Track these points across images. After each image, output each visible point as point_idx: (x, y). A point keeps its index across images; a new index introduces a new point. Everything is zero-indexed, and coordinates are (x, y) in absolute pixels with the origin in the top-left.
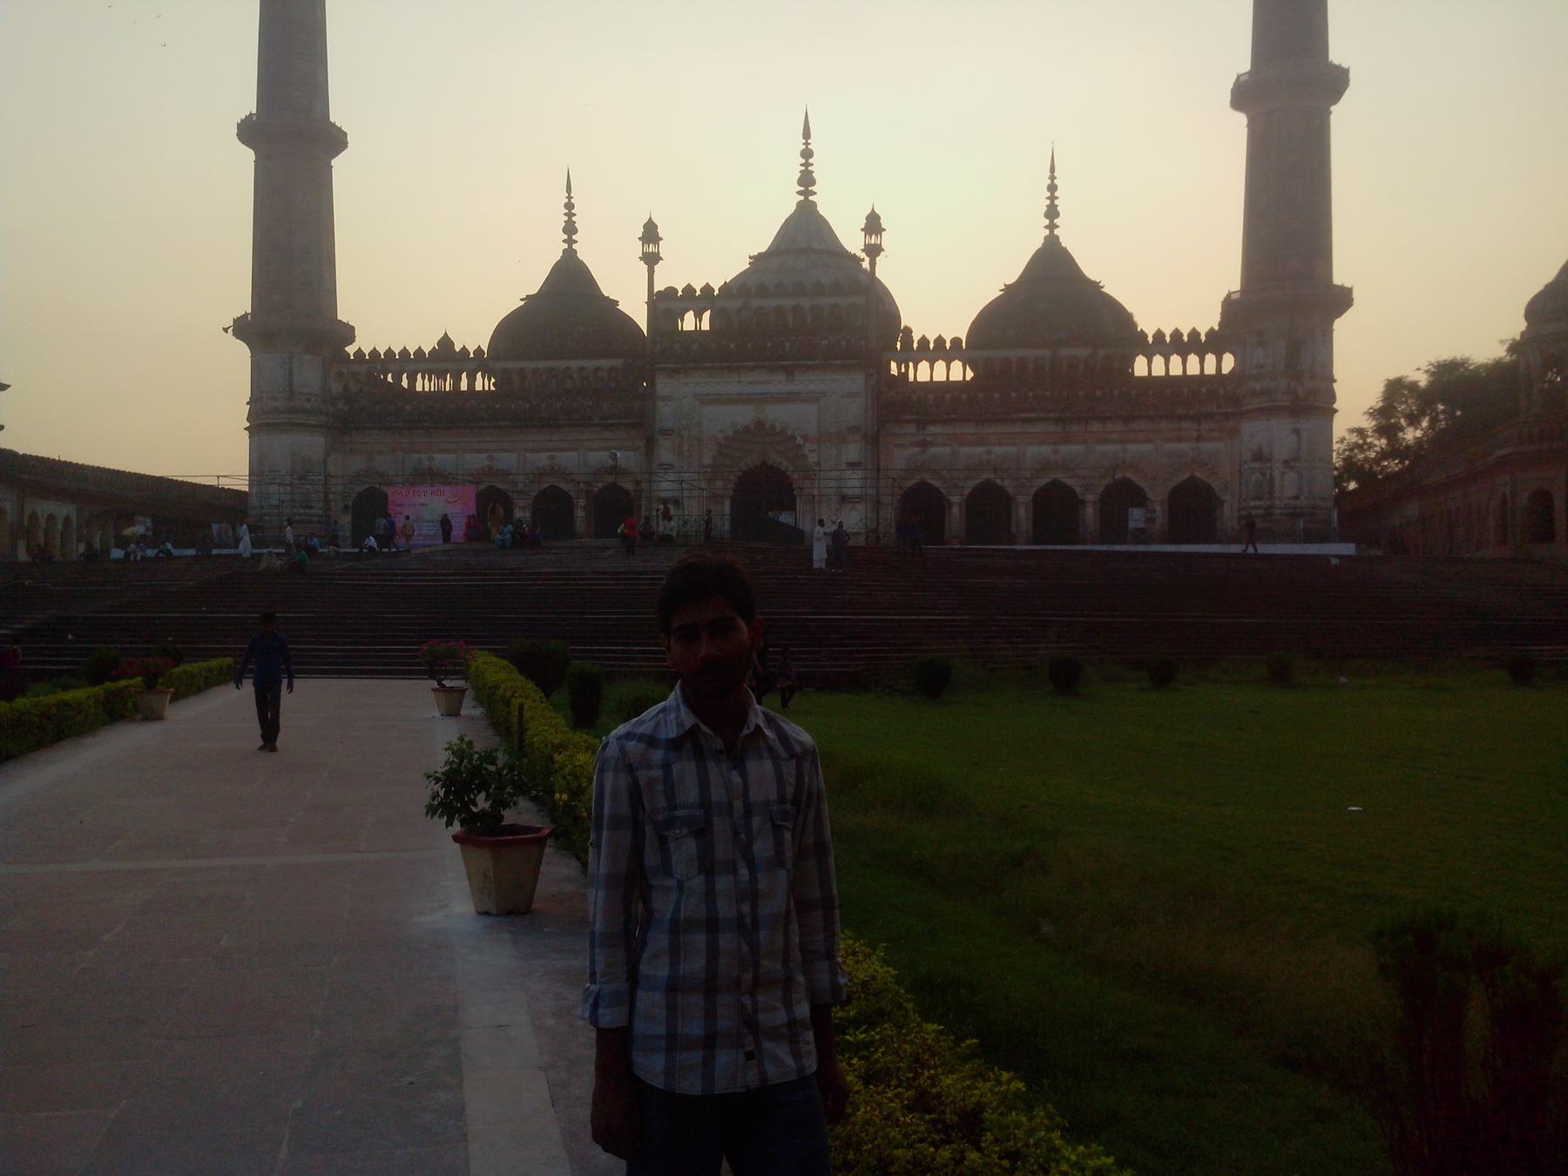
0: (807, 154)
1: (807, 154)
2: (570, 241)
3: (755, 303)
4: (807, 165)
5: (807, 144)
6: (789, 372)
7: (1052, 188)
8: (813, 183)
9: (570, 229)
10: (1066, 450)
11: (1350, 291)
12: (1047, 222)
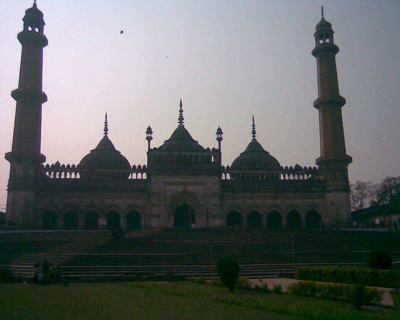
0: (181, 111)
1: (181, 111)
2: (106, 134)
3: (183, 154)
4: (181, 114)
5: (181, 108)
6: (194, 175)
7: (254, 125)
8: (183, 119)
9: (106, 130)
10: (278, 201)
11: (351, 158)
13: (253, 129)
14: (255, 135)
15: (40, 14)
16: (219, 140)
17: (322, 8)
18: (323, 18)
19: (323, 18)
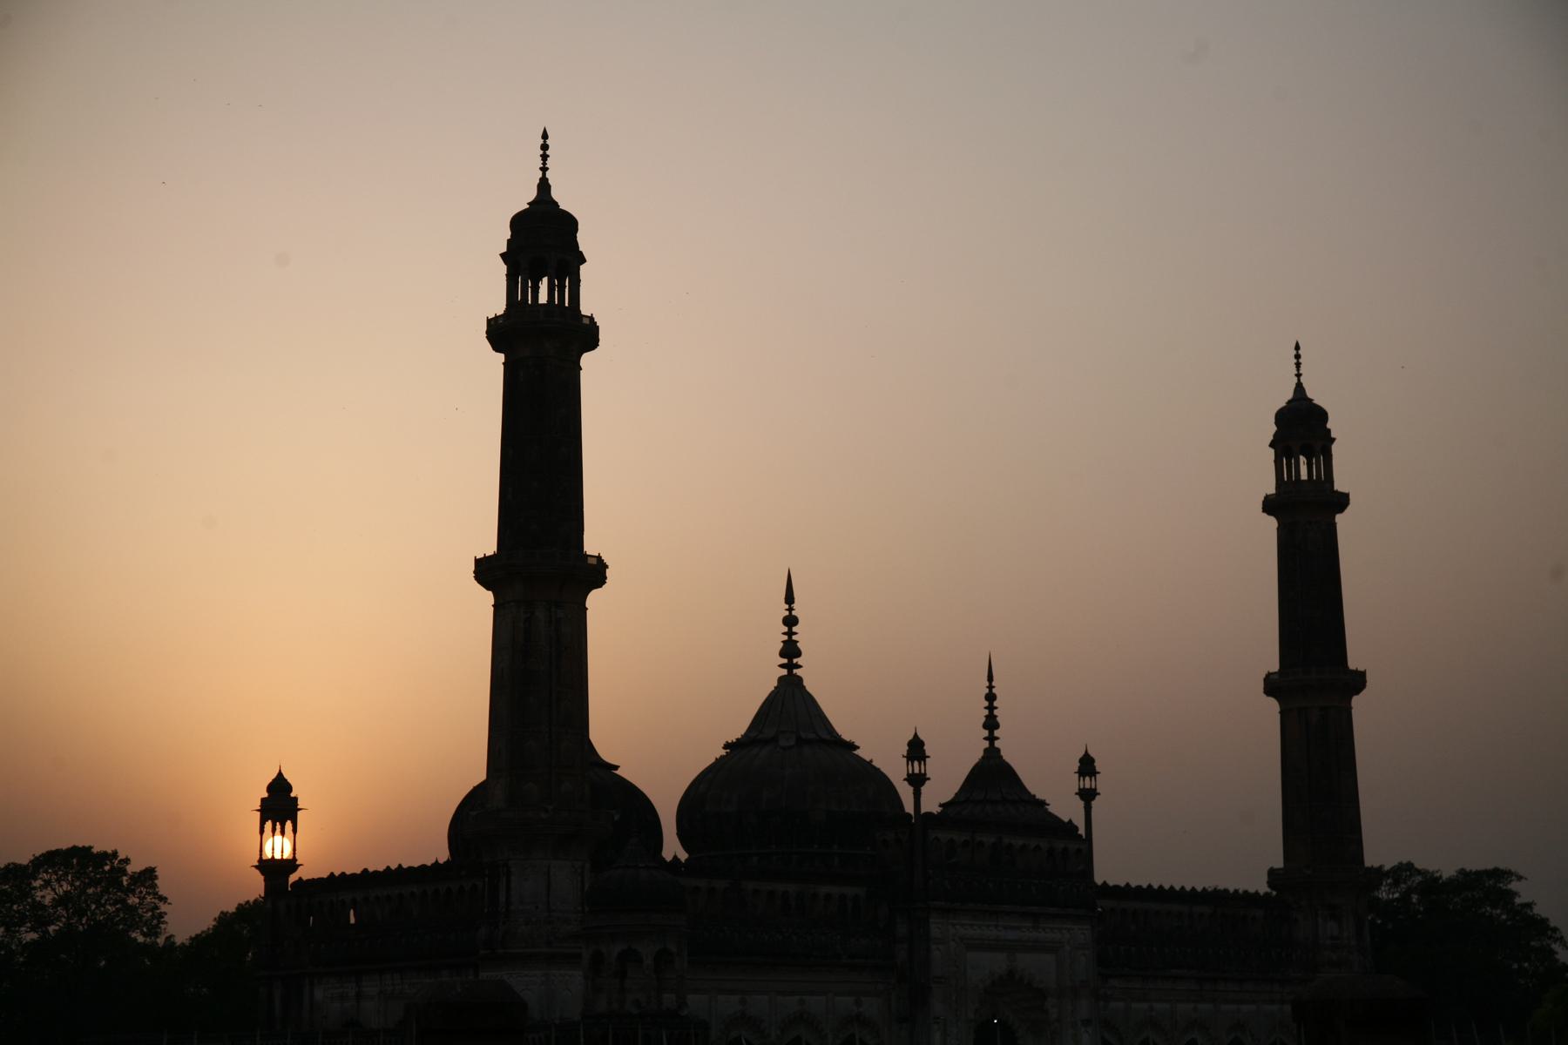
0: (791, 621)
1: (791, 621)
4: (790, 633)
5: (790, 610)
7: (991, 697)
8: (798, 654)
12: (986, 733)
14: (996, 733)
15: (568, 224)
16: (1088, 795)
17: (1297, 347)
18: (1299, 387)
19: (1299, 387)
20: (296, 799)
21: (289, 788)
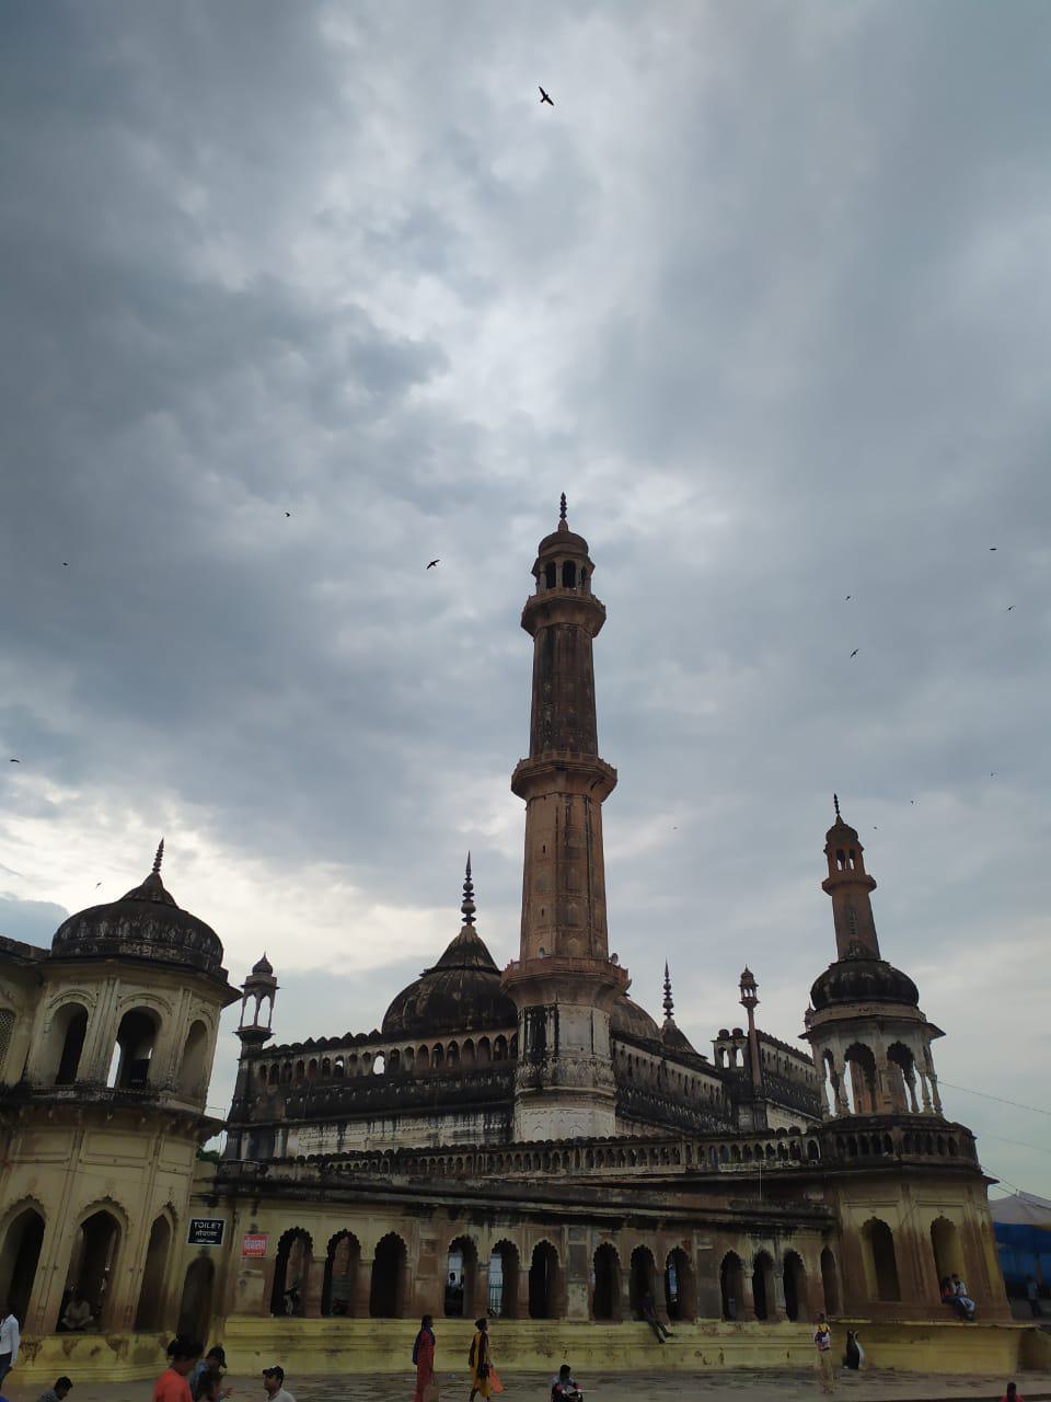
2: (469, 920)
7: (667, 987)
12: (665, 1010)
13: (665, 996)
14: (672, 1010)
17: (835, 797)
18: (839, 819)
19: (839, 819)
20: (275, 979)
21: (270, 970)
